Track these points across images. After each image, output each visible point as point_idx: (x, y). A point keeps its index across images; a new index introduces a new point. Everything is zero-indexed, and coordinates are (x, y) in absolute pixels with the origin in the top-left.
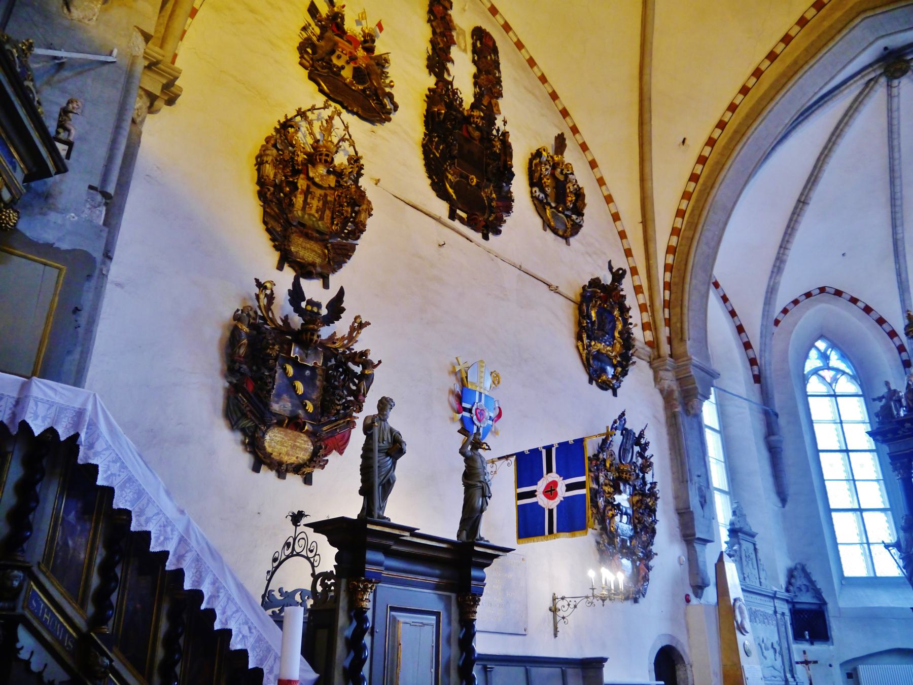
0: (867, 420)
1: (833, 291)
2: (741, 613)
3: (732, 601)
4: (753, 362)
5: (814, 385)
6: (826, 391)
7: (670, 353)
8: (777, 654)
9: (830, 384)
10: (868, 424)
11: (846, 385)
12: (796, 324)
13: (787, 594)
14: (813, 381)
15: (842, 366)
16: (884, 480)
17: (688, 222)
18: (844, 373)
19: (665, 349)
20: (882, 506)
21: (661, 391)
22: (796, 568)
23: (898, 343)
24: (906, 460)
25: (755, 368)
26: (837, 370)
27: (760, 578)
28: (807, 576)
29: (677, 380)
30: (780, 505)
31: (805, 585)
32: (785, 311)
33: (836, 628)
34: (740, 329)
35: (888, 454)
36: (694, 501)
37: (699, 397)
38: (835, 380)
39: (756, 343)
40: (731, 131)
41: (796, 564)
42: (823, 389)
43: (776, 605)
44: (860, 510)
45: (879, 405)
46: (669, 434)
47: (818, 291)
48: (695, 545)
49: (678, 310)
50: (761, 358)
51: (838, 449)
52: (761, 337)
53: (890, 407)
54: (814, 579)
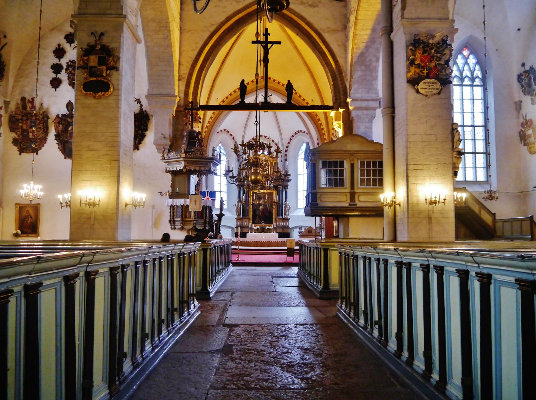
17: (213, 121)
40: (229, 100)
44: (221, 192)
49: (206, 144)
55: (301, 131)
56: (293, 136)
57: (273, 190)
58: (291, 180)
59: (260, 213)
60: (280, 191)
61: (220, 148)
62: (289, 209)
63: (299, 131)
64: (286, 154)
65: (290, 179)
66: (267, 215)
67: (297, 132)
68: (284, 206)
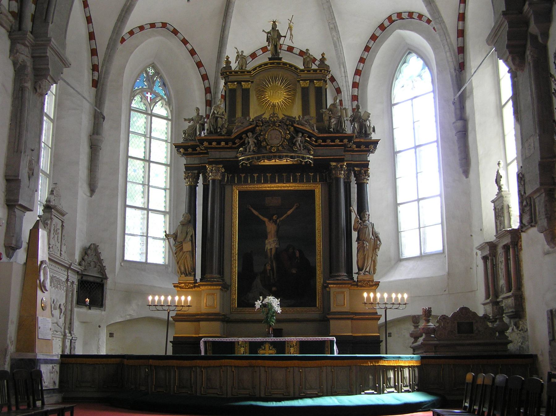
0: (169, 141)
1: (172, 29)
2: (45, 274)
3: (39, 263)
4: (95, 68)
5: (137, 103)
6: (144, 109)
7: (31, 30)
8: (62, 314)
9: (150, 105)
10: (169, 144)
11: (160, 109)
12: (137, 46)
13: (79, 267)
14: (138, 98)
15: (162, 93)
16: (170, 189)
18: (162, 98)
19: (28, 24)
20: (163, 209)
21: (15, 64)
22: (89, 248)
23: (207, 86)
24: (196, 172)
25: (96, 73)
26: (157, 95)
27: (61, 250)
28: (97, 254)
29: (33, 57)
30: (89, 194)
31: (94, 262)
32: (131, 33)
33: (110, 297)
34: (92, 36)
35: (184, 164)
36: (24, 172)
37: (49, 78)
38: (153, 102)
39: (101, 52)
41: (91, 244)
42: (142, 107)
43: (69, 274)
44: (148, 210)
45: (187, 125)
46: (13, 105)
47: (161, 25)
48: (16, 210)
50: (102, 67)
51: (142, 158)
52: (107, 48)
53: (196, 129)
54: (102, 258)
55: (399, 15)
56: (374, 37)
57: (315, 181)
58: (376, 143)
59: (268, 268)
60: (338, 180)
61: (150, 81)
62: (376, 247)
63: (394, 17)
64: (356, 94)
65: (374, 137)
66: (294, 271)
67: (387, 23)
68: (355, 235)
